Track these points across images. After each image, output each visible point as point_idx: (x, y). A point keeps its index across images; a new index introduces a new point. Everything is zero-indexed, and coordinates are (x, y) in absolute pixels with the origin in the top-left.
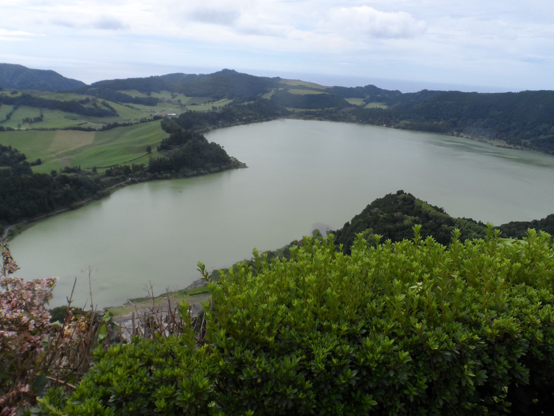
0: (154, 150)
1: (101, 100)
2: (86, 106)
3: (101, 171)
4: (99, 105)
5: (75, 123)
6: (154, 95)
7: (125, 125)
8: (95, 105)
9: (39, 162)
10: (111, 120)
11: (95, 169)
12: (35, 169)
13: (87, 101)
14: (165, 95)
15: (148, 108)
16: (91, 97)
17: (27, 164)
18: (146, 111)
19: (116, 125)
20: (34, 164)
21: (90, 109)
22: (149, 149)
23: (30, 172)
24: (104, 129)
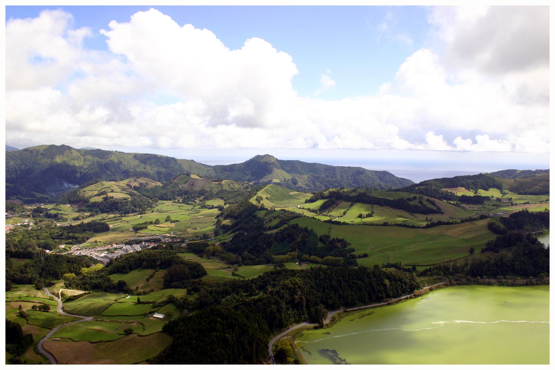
0: (477, 252)
1: (426, 197)
2: (412, 203)
3: (420, 269)
4: (425, 202)
5: (400, 220)
6: (482, 193)
7: (448, 223)
8: (421, 202)
9: (365, 256)
10: (436, 218)
11: (414, 268)
12: (360, 262)
13: (415, 198)
14: (494, 193)
15: (476, 207)
16: (418, 196)
17: (354, 257)
18: (473, 210)
19: (440, 223)
20: (360, 257)
21: (415, 207)
22: (472, 251)
23: (356, 264)
24: (427, 227)
